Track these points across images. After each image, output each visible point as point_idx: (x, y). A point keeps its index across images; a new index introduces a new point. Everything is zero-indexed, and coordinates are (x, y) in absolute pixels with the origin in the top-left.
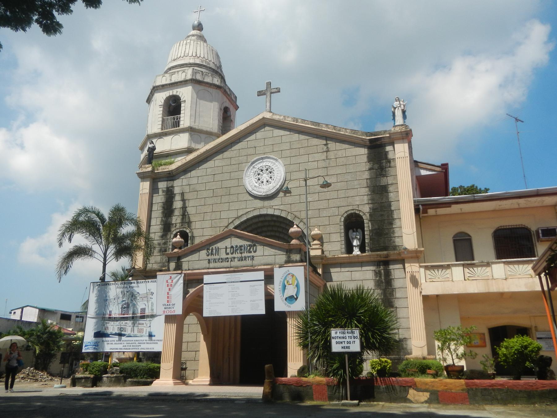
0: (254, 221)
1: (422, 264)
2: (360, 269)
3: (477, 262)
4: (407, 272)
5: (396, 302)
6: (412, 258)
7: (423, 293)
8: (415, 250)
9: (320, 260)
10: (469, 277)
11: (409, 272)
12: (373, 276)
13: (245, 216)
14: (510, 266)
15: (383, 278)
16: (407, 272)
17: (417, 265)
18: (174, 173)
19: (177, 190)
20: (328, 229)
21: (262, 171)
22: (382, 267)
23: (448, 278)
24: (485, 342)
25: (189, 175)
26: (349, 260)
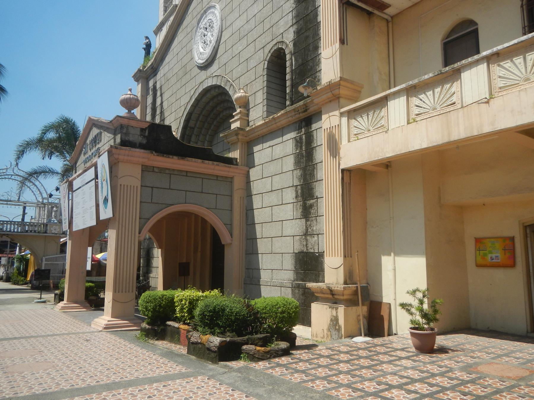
0: (205, 100)
1: (343, 110)
2: (279, 140)
3: (431, 75)
4: (325, 129)
5: (317, 189)
6: (330, 101)
7: (342, 166)
8: (328, 85)
9: (235, 138)
10: (417, 115)
11: (327, 129)
12: (294, 148)
13: (194, 96)
14: (501, 64)
15: (304, 147)
16: (325, 129)
17: (337, 113)
18: (155, 66)
19: (158, 86)
20: (254, 86)
21: (206, 29)
22: (303, 130)
23: (383, 126)
24: (513, 257)
25: (164, 63)
26: (267, 129)
